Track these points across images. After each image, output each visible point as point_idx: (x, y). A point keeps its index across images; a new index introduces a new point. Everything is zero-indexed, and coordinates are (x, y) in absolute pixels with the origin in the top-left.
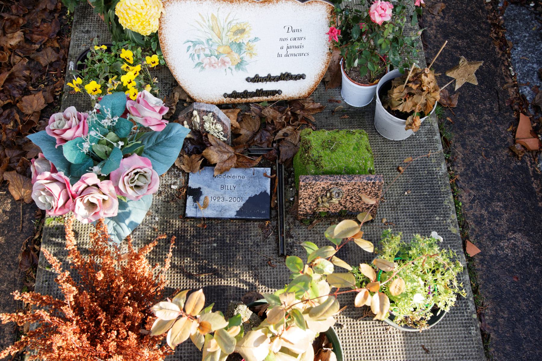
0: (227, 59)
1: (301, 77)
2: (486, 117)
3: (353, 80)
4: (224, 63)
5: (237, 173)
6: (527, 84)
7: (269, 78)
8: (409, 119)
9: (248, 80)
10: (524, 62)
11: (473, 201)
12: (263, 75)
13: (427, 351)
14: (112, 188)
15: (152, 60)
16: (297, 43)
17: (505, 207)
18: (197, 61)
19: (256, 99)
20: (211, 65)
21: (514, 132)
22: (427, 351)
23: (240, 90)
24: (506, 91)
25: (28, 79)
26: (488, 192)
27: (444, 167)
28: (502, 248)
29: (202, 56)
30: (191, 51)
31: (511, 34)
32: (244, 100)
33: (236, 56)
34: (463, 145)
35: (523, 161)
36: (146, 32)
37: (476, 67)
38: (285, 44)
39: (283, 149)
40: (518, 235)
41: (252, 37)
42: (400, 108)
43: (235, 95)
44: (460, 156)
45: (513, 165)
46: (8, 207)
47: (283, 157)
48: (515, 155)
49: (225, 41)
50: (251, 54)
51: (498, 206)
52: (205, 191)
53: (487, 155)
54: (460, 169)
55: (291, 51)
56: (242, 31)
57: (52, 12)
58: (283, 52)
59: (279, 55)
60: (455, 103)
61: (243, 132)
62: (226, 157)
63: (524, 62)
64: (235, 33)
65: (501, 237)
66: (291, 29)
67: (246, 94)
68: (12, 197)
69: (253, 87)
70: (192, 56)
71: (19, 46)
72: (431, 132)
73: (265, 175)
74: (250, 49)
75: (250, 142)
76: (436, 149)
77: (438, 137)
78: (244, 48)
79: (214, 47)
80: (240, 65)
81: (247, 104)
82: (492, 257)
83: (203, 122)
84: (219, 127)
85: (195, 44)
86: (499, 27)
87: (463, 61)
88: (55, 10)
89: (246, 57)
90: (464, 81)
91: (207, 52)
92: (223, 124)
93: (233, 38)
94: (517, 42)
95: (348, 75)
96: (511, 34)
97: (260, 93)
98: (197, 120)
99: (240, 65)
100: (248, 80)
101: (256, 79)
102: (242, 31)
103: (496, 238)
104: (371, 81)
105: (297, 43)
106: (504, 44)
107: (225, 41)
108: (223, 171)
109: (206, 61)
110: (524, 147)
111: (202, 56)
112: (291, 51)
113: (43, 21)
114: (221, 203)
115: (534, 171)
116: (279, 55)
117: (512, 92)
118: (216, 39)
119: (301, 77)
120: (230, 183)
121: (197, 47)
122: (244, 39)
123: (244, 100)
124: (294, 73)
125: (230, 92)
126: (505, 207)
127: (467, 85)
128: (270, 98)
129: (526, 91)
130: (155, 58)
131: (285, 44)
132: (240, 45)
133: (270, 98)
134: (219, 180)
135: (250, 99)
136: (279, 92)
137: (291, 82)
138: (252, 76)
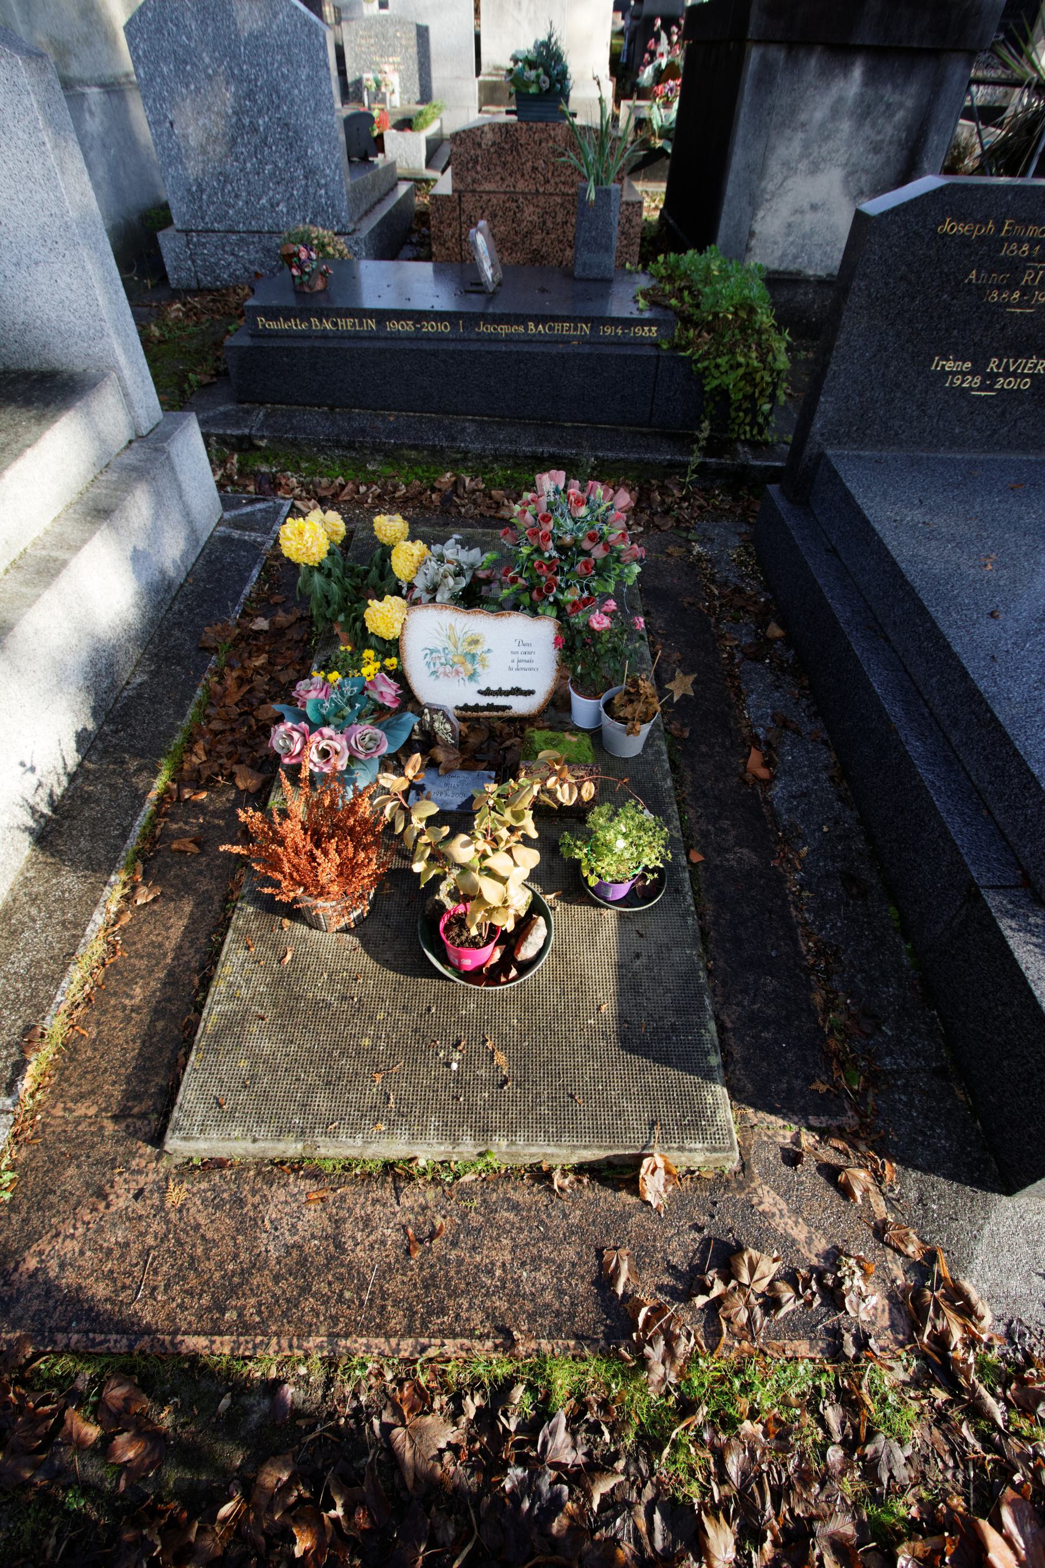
0: (461, 669)
1: (530, 693)
2: (717, 749)
3: (579, 694)
4: (457, 673)
5: (464, 775)
6: (761, 726)
7: (500, 692)
8: (630, 724)
9: (480, 692)
10: (759, 707)
11: (700, 817)
12: (494, 688)
13: (641, 936)
14: (345, 743)
15: (391, 662)
16: (527, 657)
17: (733, 825)
18: (432, 669)
19: (486, 713)
20: (446, 674)
21: (745, 764)
22: (641, 936)
23: (472, 704)
24: (739, 730)
25: (267, 692)
26: (716, 811)
27: (669, 783)
28: (728, 860)
29: (438, 665)
30: (428, 659)
31: (747, 684)
32: (475, 714)
33: (469, 666)
34: (693, 770)
35: (753, 788)
36: (389, 635)
37: (691, 678)
38: (515, 657)
39: (509, 756)
40: (745, 851)
41: (485, 649)
42: (621, 714)
43: (466, 708)
44: (689, 778)
45: (743, 791)
46: (232, 796)
47: (508, 763)
48: (745, 782)
49: (460, 650)
50: (484, 666)
51: (726, 824)
52: (429, 787)
53: (717, 780)
54: (688, 789)
55: (522, 665)
56: (476, 642)
57: (296, 642)
58: (514, 665)
59: (510, 669)
60: (686, 734)
61: (471, 740)
62: (452, 757)
63: (759, 707)
64: (470, 644)
65: (727, 850)
66: (521, 643)
67: (477, 708)
68: (237, 787)
69: (484, 701)
70: (428, 664)
71: (262, 667)
72: (659, 753)
73: (490, 777)
74: (483, 660)
75: (479, 750)
76: (662, 767)
77: (665, 757)
78: (478, 658)
79: (450, 656)
80: (472, 676)
81: (478, 719)
82: (716, 866)
83: (433, 721)
84: (448, 726)
85: (432, 652)
86: (734, 677)
87: (678, 673)
88: (301, 641)
89: (479, 668)
90: (681, 692)
91: (443, 660)
92: (452, 724)
93: (468, 649)
94: (752, 691)
95: (576, 691)
96: (747, 684)
97: (491, 707)
98: (428, 718)
99: (472, 676)
100: (480, 692)
101: (487, 692)
102: (476, 642)
103: (721, 850)
104: (595, 696)
105: (527, 657)
106: (739, 692)
107: (460, 650)
108: (448, 771)
109: (441, 669)
110: (755, 776)
111: (438, 665)
112: (522, 665)
113: (288, 649)
114: (443, 797)
115: (765, 798)
116: (510, 669)
117: (745, 731)
118: (452, 648)
119: (530, 693)
120: (454, 782)
121: (434, 655)
122: (478, 650)
123: (475, 714)
124: (524, 688)
125: (461, 705)
126: (733, 825)
127: (684, 696)
128: (500, 713)
129: (760, 731)
130: (394, 660)
131: (515, 657)
132: (474, 656)
133: (500, 713)
134: (444, 780)
135: (480, 714)
136: (509, 708)
137: (521, 698)
138: (484, 689)
